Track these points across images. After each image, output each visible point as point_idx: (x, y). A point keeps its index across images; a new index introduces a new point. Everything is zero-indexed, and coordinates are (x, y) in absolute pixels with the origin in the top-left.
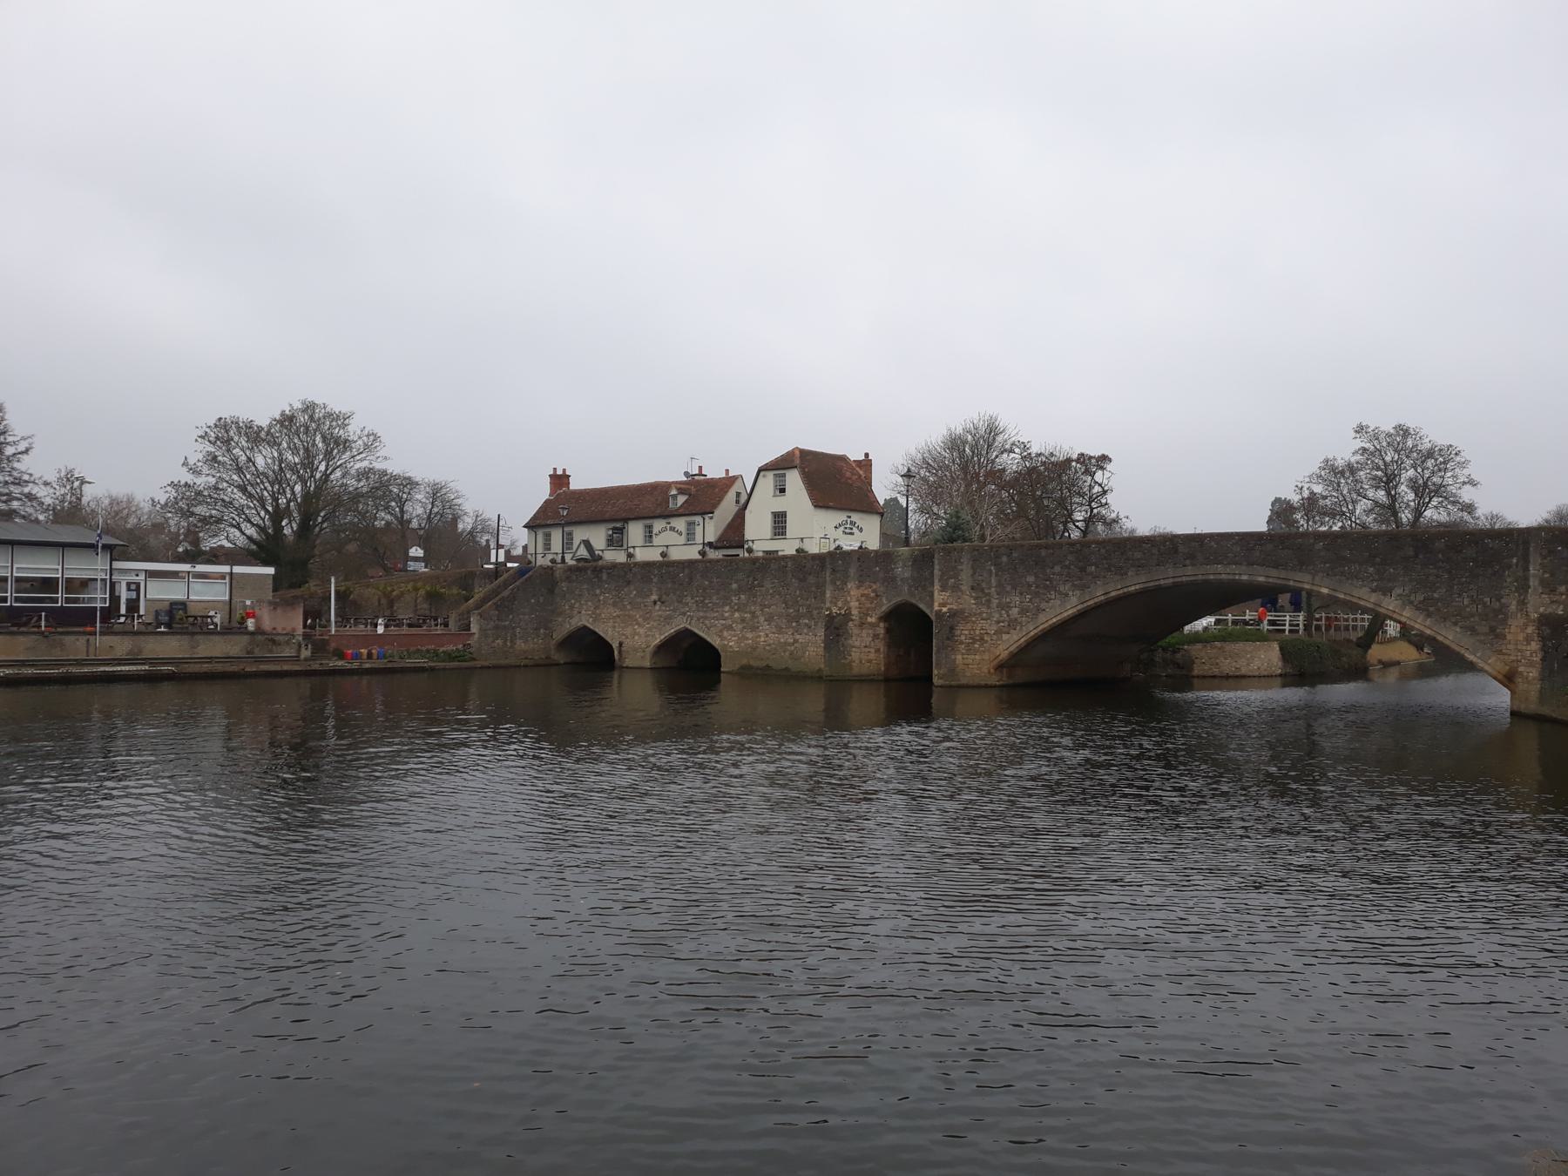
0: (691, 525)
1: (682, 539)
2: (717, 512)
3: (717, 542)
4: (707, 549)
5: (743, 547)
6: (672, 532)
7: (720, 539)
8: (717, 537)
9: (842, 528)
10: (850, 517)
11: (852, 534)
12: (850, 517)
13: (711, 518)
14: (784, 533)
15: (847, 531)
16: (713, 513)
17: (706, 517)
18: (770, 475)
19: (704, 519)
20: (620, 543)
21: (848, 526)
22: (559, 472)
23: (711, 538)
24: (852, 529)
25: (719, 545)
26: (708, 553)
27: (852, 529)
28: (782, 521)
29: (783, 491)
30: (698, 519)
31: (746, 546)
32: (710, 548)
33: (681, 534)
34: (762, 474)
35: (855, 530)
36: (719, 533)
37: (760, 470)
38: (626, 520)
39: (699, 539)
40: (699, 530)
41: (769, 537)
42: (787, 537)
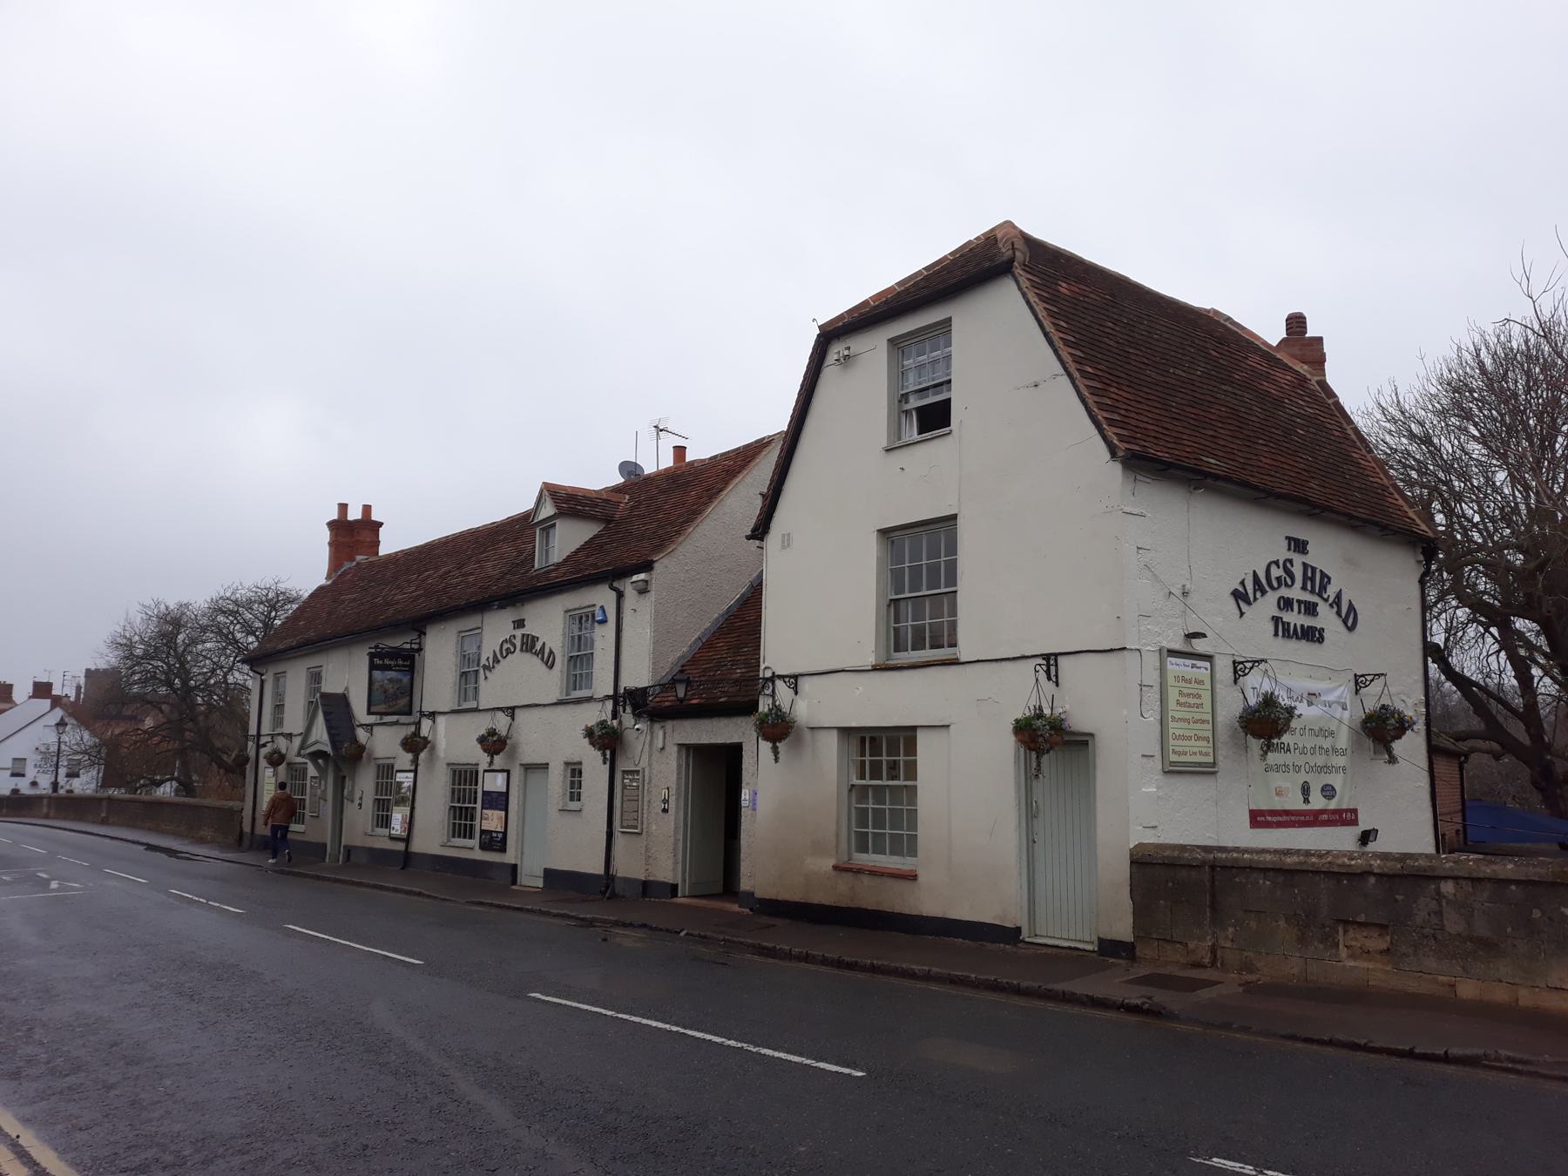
0: (585, 619)
1: (550, 684)
2: (667, 568)
3: (668, 686)
4: (628, 718)
5: (749, 708)
6: (527, 656)
7: (683, 674)
8: (665, 671)
9: (1272, 598)
10: (1299, 546)
11: (1312, 635)
12: (1299, 546)
13: (643, 590)
14: (944, 636)
15: (1295, 618)
16: (647, 566)
17: (628, 586)
18: (873, 348)
19: (620, 595)
20: (403, 702)
21: (1296, 593)
22: (354, 514)
23: (638, 675)
24: (1311, 609)
25: (668, 700)
26: (630, 736)
27: (1311, 609)
28: (934, 570)
29: (935, 418)
30: (602, 597)
31: (764, 705)
32: (637, 716)
33: (549, 663)
34: (836, 351)
35: (1326, 618)
36: (681, 648)
37: (830, 335)
38: (420, 624)
39: (603, 684)
40: (603, 638)
41: (870, 660)
42: (965, 651)
